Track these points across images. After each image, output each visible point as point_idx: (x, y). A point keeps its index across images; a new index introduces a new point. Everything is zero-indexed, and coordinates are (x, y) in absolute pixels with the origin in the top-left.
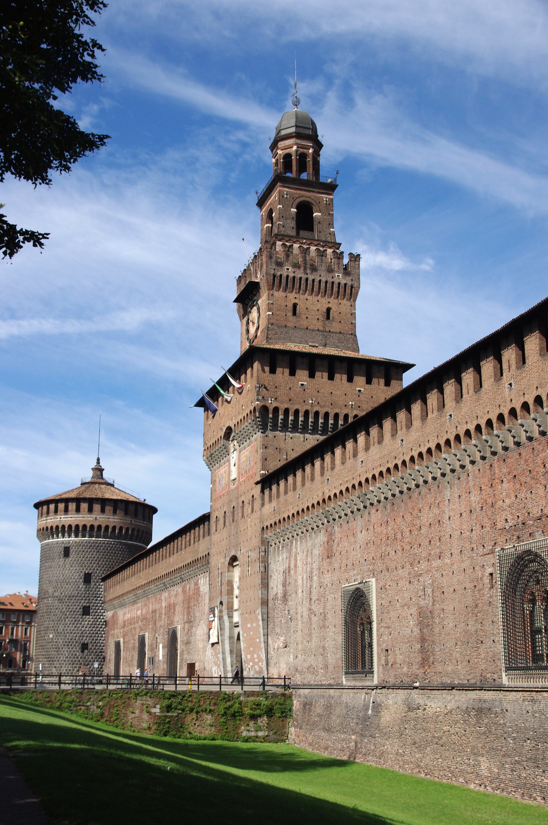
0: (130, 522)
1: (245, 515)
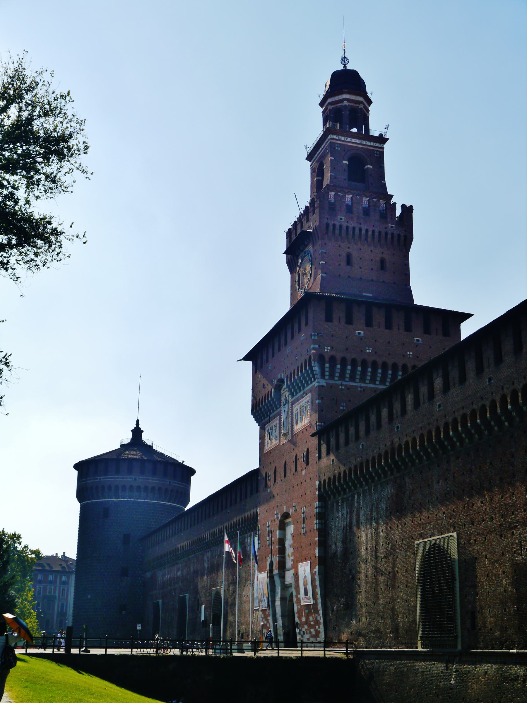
0: (168, 483)
1: (299, 469)
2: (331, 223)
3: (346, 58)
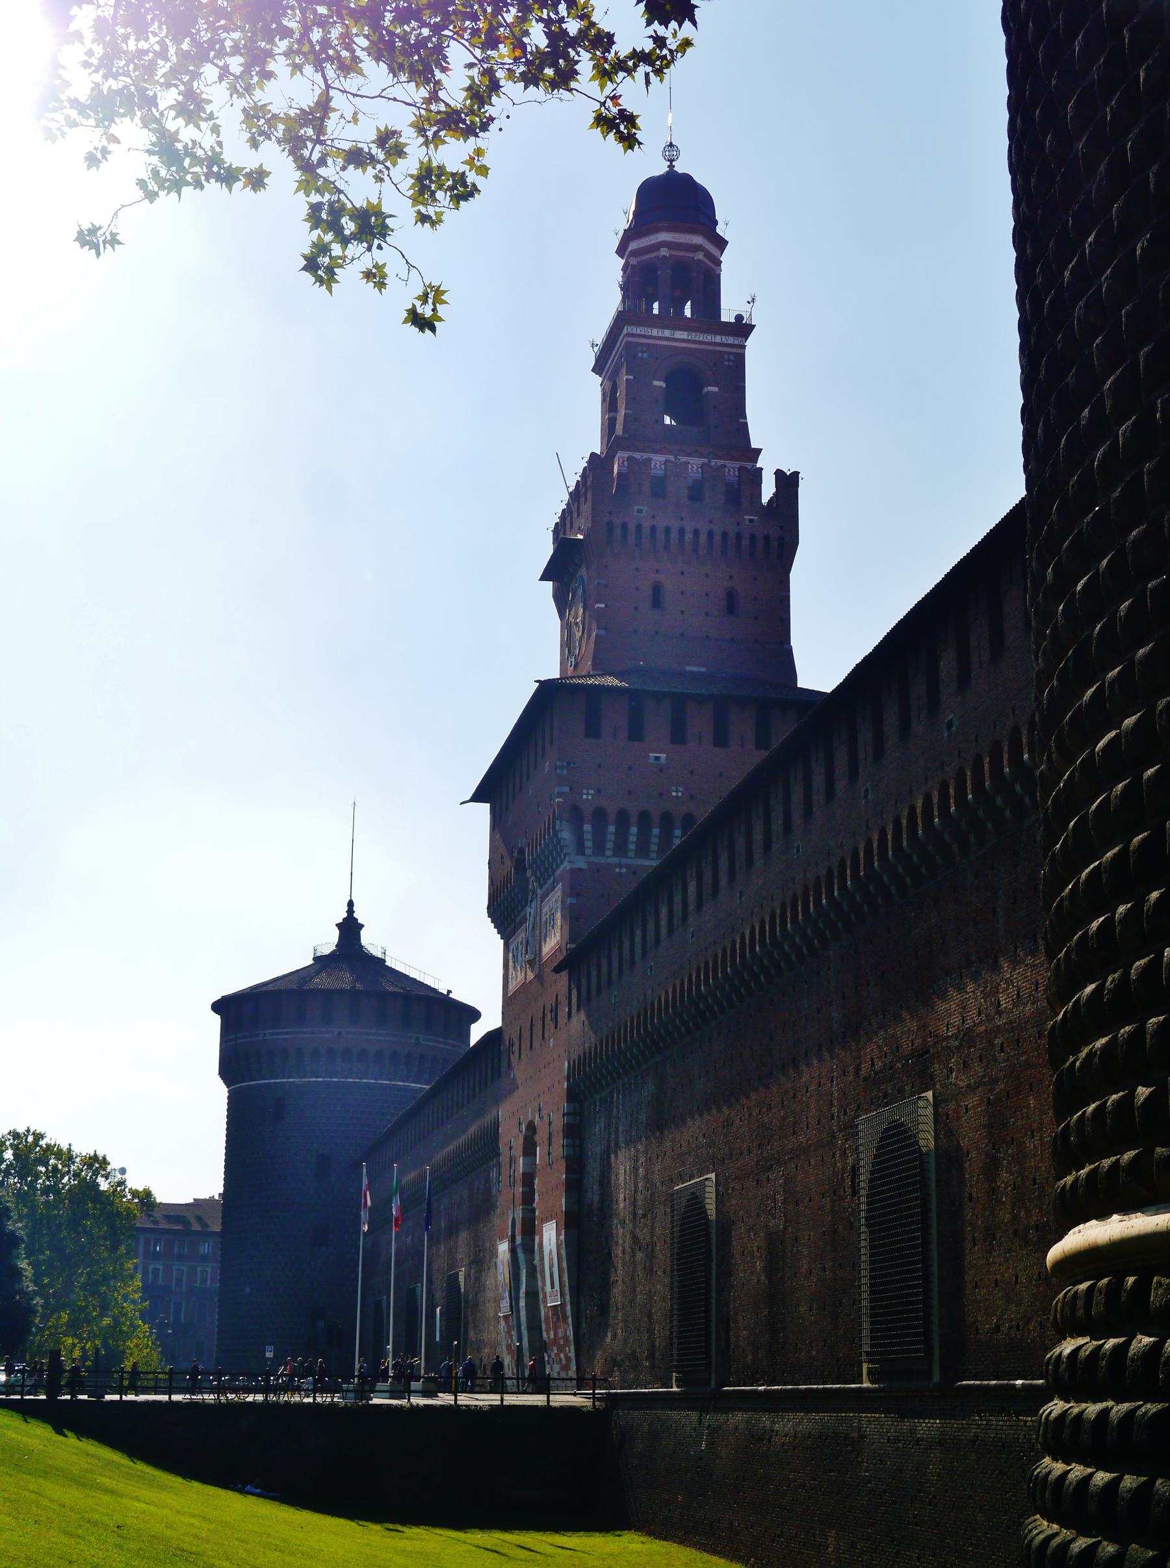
0: (413, 1041)
1: (547, 1035)
2: (618, 522)
3: (673, 146)
